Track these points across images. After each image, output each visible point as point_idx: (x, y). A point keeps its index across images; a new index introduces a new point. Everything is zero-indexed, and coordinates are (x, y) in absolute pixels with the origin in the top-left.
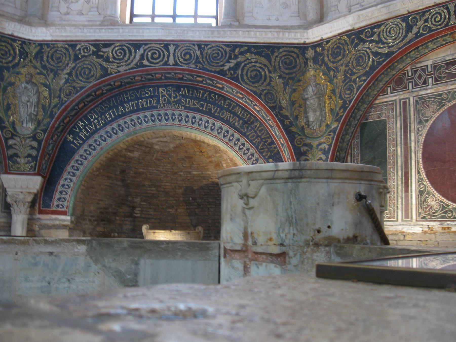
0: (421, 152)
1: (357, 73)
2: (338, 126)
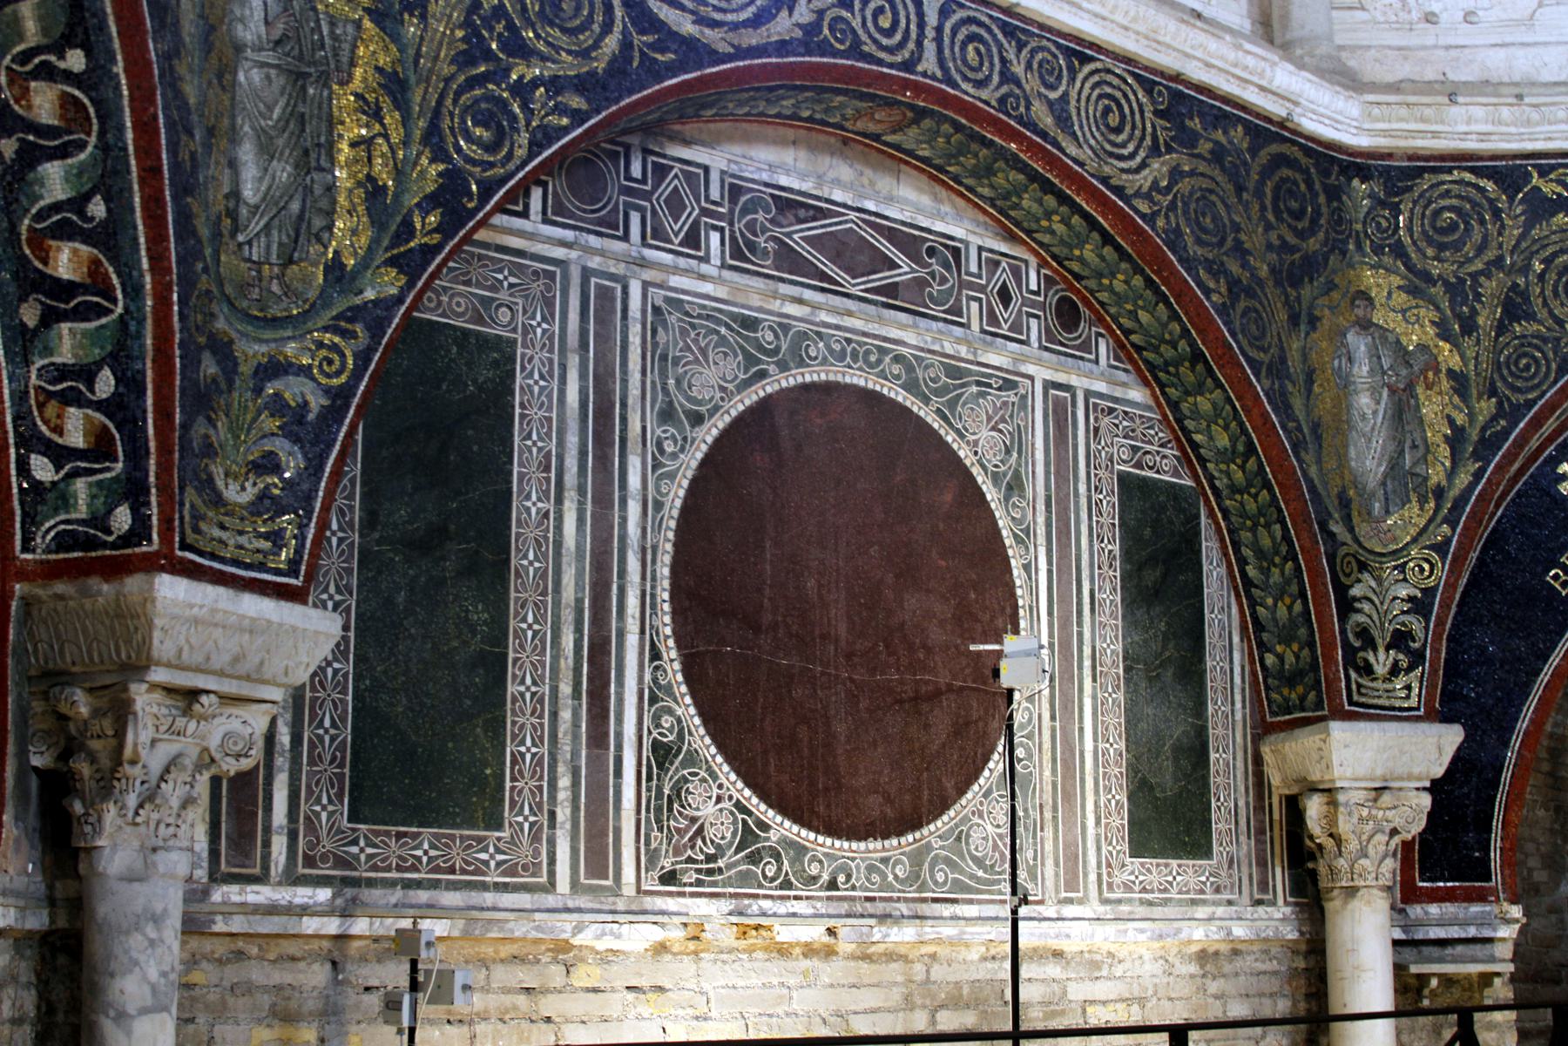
0: (667, 559)
1: (544, 58)
2: (400, 300)
